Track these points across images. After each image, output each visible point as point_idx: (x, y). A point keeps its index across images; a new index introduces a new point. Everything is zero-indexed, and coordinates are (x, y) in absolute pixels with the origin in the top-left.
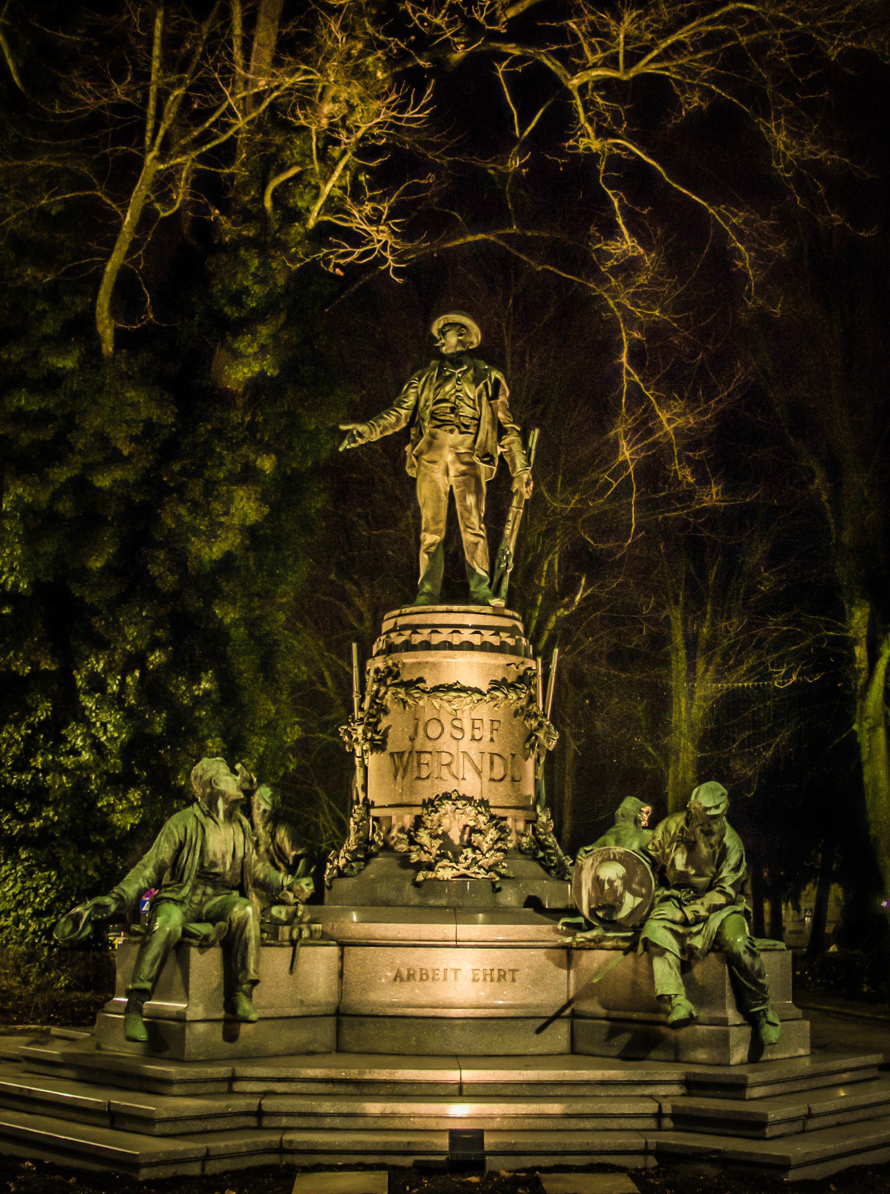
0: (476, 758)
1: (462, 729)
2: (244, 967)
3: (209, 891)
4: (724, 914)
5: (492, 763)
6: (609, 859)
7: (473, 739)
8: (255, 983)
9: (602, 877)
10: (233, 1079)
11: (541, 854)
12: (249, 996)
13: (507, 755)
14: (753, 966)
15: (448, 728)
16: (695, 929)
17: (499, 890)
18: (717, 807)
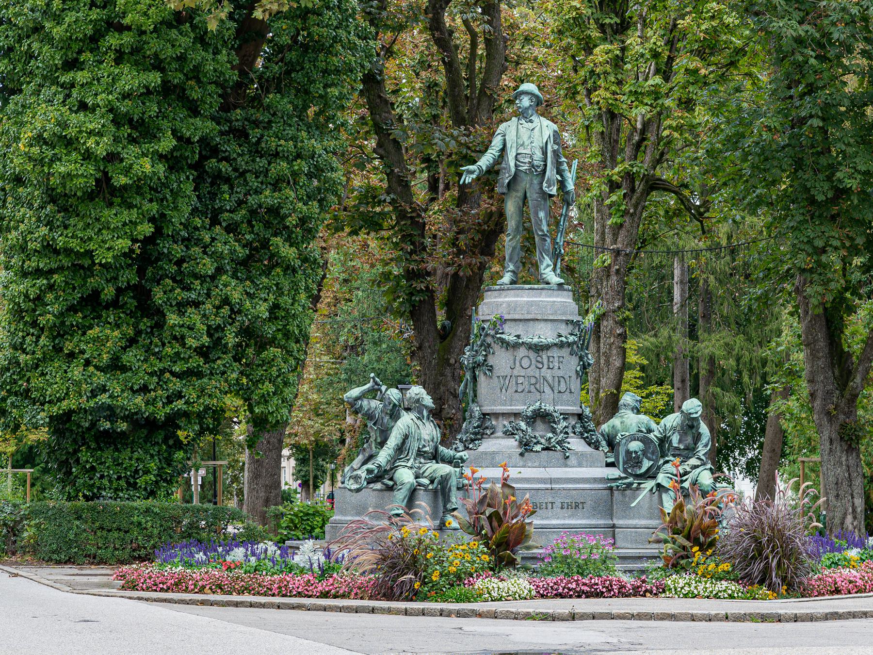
0: (550, 379)
1: (542, 364)
3: (422, 460)
4: (698, 470)
5: (559, 382)
6: (635, 440)
7: (549, 368)
9: (631, 450)
11: (586, 435)
16: (684, 478)
17: (568, 457)
18: (696, 413)
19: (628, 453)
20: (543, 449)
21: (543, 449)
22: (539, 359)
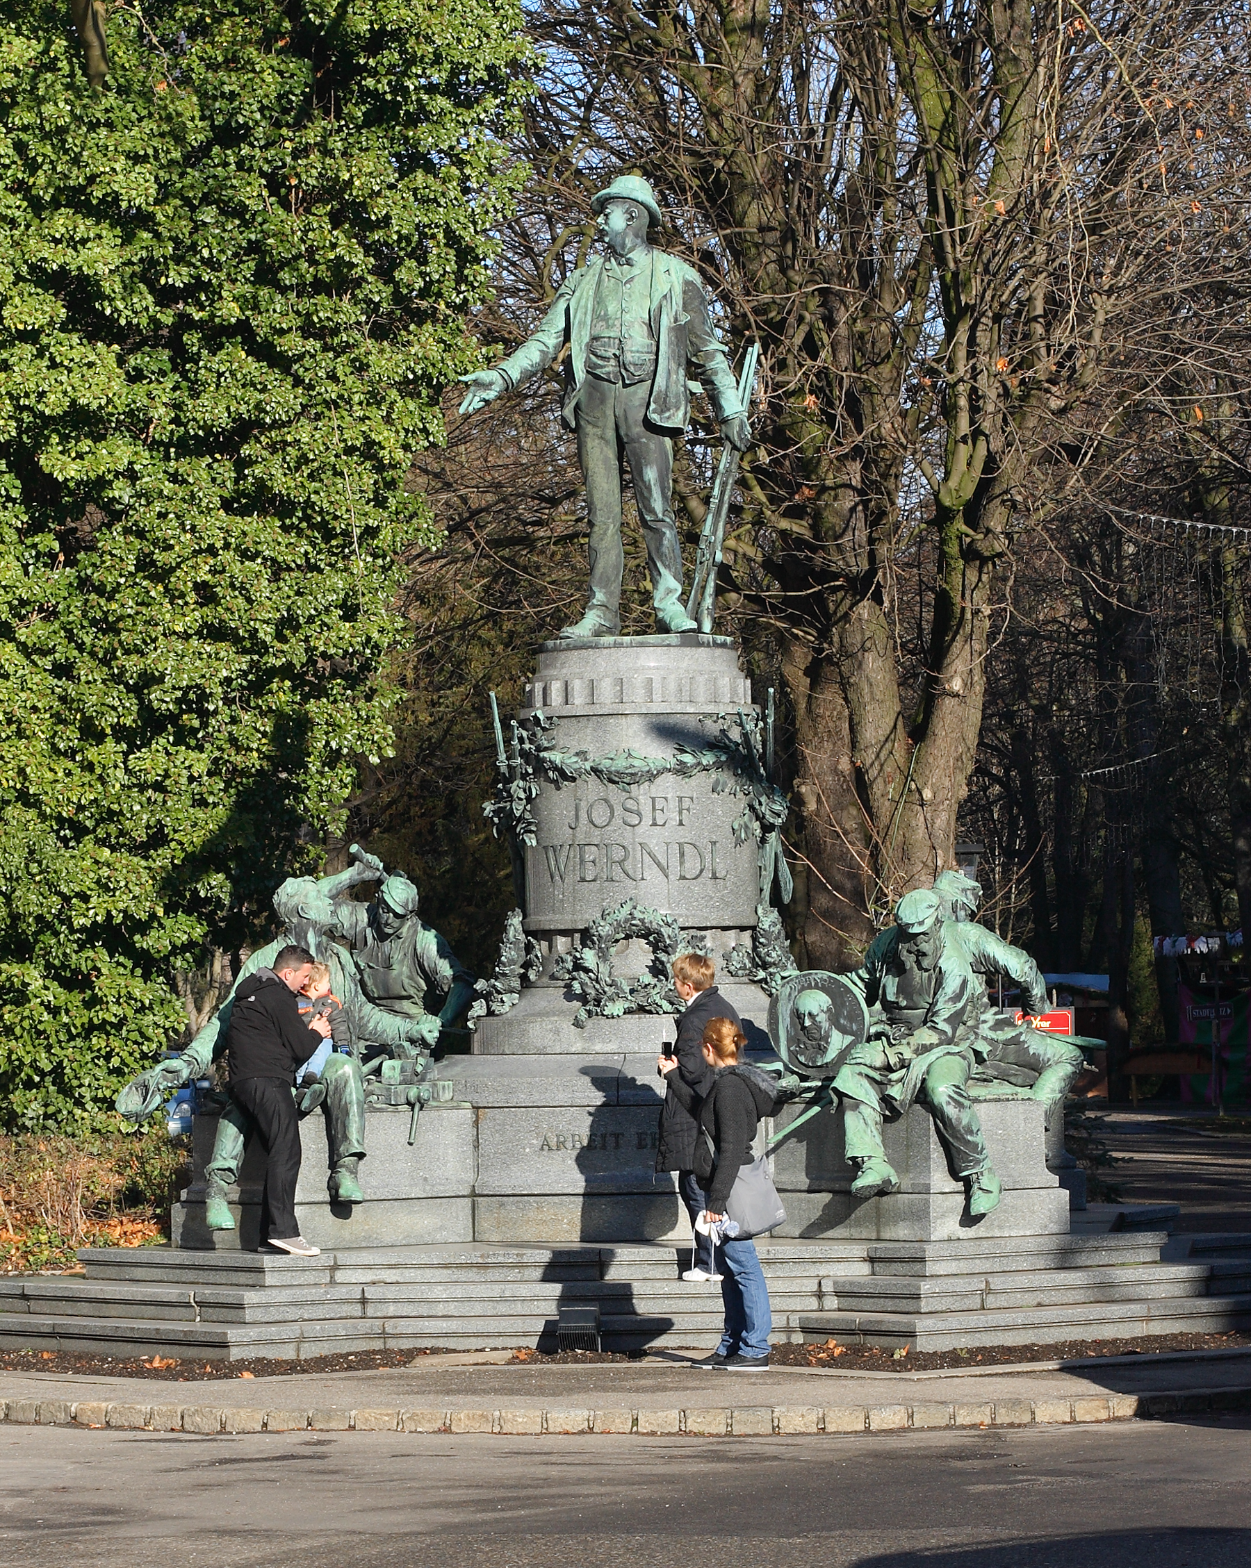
1: (639, 814)
2: (346, 1138)
5: (682, 855)
6: (810, 987)
8: (361, 1156)
9: (802, 1010)
10: (335, 1268)
11: (762, 974)
12: (354, 1173)
13: (704, 843)
14: (959, 1119)
15: (618, 811)
18: (921, 923)
19: (798, 1016)
20: (628, 1012)
21: (628, 1012)
22: (630, 804)
